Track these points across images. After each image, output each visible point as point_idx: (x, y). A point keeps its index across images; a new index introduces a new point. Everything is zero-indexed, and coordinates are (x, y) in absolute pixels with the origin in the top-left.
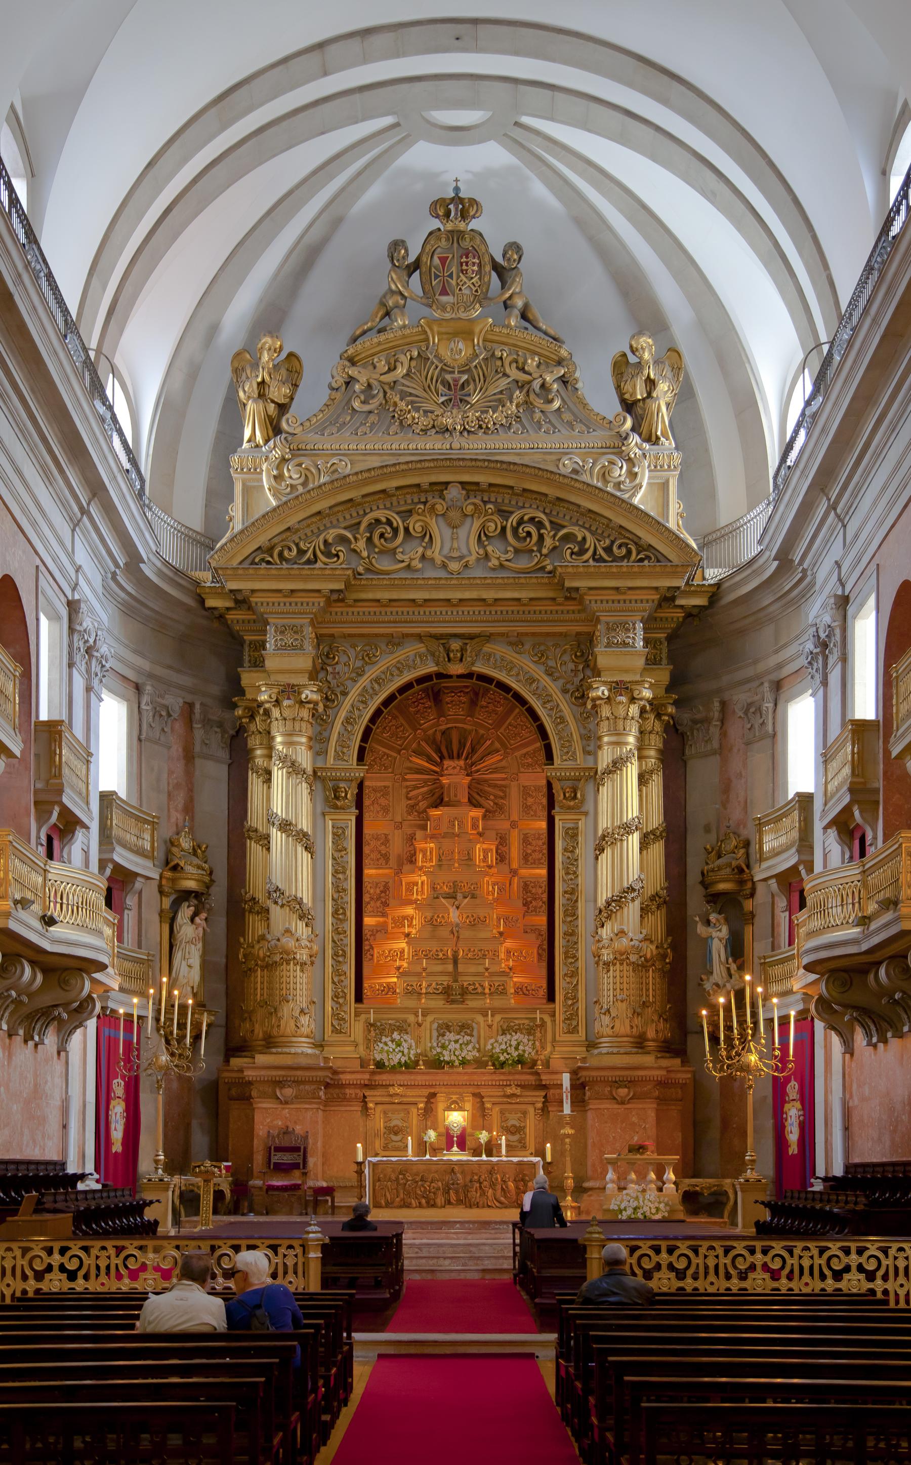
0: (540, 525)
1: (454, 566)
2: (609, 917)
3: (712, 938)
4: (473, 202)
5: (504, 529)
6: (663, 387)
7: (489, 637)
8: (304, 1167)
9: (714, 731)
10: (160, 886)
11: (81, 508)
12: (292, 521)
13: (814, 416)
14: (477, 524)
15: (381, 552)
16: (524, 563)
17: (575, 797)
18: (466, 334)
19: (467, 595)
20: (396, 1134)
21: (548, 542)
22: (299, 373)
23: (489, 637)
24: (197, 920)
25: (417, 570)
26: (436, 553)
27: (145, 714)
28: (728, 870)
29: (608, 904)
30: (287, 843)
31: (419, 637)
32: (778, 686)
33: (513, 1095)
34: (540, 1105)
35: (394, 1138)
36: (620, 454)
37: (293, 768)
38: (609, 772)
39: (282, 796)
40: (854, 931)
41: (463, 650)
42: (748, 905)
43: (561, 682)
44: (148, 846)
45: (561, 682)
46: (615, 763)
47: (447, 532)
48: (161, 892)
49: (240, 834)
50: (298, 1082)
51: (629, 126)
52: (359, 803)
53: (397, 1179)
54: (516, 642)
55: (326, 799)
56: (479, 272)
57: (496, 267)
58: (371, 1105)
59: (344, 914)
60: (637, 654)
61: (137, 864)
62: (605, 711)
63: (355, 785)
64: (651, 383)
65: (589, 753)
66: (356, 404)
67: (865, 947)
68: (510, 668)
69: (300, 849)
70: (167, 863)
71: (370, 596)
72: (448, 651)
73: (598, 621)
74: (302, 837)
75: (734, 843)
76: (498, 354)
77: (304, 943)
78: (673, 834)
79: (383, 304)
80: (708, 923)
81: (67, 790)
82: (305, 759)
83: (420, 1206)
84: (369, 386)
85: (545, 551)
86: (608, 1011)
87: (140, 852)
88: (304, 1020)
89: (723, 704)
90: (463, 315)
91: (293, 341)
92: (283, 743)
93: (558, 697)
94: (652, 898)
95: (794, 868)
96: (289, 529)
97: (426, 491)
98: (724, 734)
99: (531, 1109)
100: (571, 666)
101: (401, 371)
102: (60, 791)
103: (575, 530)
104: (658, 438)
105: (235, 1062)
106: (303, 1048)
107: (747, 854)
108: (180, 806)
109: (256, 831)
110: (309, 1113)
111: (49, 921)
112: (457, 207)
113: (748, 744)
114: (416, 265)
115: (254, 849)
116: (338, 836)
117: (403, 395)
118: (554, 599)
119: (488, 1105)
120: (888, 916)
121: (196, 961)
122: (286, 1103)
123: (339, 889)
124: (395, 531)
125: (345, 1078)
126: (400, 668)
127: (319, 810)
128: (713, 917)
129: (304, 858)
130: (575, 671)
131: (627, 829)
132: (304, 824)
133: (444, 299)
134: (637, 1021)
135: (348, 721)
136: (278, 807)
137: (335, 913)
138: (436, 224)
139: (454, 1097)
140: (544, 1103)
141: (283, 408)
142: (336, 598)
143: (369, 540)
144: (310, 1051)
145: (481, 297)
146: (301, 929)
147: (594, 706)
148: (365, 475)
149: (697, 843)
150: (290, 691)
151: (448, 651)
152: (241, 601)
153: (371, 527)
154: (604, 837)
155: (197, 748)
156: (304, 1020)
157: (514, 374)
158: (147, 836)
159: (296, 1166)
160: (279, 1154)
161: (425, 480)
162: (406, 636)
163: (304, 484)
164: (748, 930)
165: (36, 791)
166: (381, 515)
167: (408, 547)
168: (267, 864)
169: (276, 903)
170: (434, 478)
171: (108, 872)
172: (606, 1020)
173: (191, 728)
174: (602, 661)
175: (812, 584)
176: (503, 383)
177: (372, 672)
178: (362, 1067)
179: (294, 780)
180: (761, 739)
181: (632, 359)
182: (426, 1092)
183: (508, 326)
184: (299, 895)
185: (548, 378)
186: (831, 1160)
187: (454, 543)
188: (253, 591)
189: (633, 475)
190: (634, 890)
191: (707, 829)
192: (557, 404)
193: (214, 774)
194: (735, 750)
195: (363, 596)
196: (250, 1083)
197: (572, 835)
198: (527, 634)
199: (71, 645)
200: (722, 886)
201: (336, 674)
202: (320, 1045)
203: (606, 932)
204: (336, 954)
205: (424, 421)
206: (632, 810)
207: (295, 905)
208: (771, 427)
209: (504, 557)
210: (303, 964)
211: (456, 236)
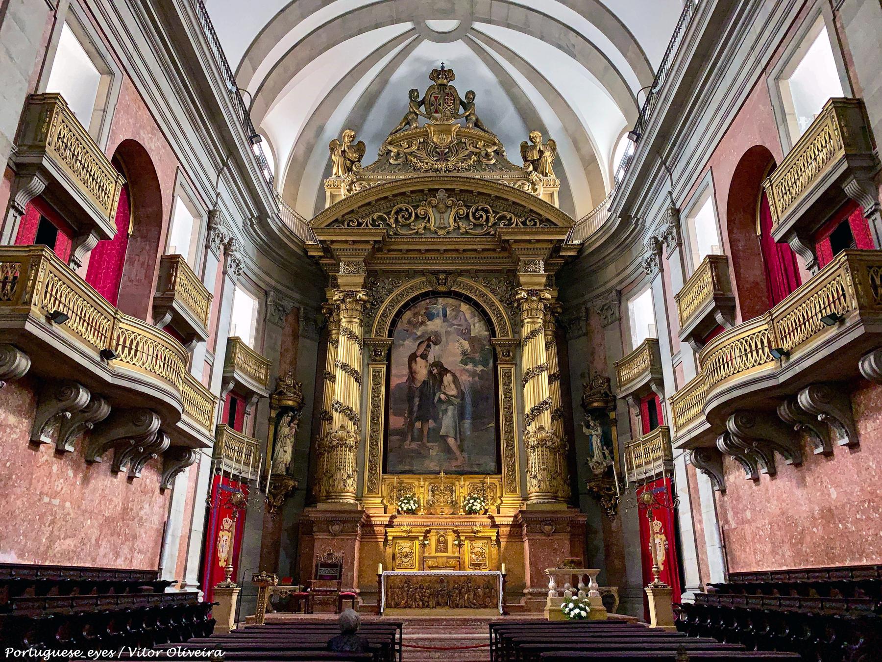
0: (487, 212)
1: (441, 232)
2: (533, 419)
3: (592, 435)
4: (450, 71)
5: (468, 214)
6: (547, 154)
7: (461, 273)
8: (340, 578)
9: (583, 323)
10: (270, 403)
11: (222, 160)
12: (355, 207)
13: (659, 93)
14: (453, 211)
15: (402, 226)
16: (479, 231)
17: (509, 356)
18: (448, 132)
19: (449, 247)
20: (406, 557)
21: (492, 220)
22: (364, 151)
23: (461, 273)
24: (292, 425)
25: (422, 234)
26: (432, 226)
27: (269, 307)
28: (599, 395)
29: (532, 411)
31: (422, 273)
32: (620, 293)
34: (494, 538)
35: (404, 560)
36: (528, 180)
37: (351, 336)
38: (528, 338)
39: (346, 351)
40: (769, 367)
41: (446, 279)
42: (612, 415)
43: (499, 296)
44: (262, 377)
45: (499, 296)
46: (532, 332)
47: (438, 216)
48: (271, 407)
49: (322, 375)
50: (344, 522)
52: (389, 357)
53: (403, 587)
54: (474, 274)
55: (370, 357)
56: (454, 103)
57: (462, 103)
58: (390, 538)
59: (378, 420)
60: (541, 275)
61: (253, 385)
62: (525, 306)
63: (386, 348)
64: (541, 152)
65: (516, 333)
66: (392, 161)
67: (782, 379)
68: (471, 288)
69: (352, 379)
70: (276, 390)
71: (396, 247)
72: (438, 279)
73: (519, 260)
74: (353, 373)
75: (601, 381)
76: (463, 140)
77: (352, 434)
78: (563, 376)
79: (406, 118)
80: (588, 427)
81: (176, 297)
82: (357, 330)
83: (418, 607)
84: (398, 154)
85: (490, 224)
86: (535, 477)
87: (257, 379)
88: (350, 481)
89: (587, 309)
90: (446, 123)
93: (497, 303)
94: (556, 411)
95: (647, 385)
96: (352, 211)
97: (426, 195)
98: (588, 325)
100: (504, 288)
101: (414, 148)
102: (172, 299)
103: (506, 213)
106: (349, 499)
107: (609, 386)
108: (288, 361)
109: (329, 373)
110: (349, 542)
111: (107, 355)
112: (442, 75)
113: (604, 327)
114: (423, 102)
115: (328, 383)
116: (376, 377)
117: (415, 157)
118: (494, 250)
119: (463, 538)
120: (833, 331)
121: (289, 449)
122: (335, 535)
123: (376, 406)
124: (410, 214)
125: (375, 520)
126: (412, 289)
127: (366, 362)
128: (591, 423)
129: (355, 385)
130: (507, 291)
131: (541, 368)
132: (356, 365)
133: (436, 115)
134: (554, 482)
135: (384, 315)
137: (372, 419)
138: (433, 83)
139: (442, 533)
140: (497, 537)
142: (379, 247)
143: (396, 220)
144: (352, 502)
145: (455, 115)
146: (351, 426)
147: (519, 305)
148: (395, 184)
149: (577, 384)
150: (353, 294)
151: (438, 279)
153: (397, 213)
154: (527, 374)
155: (300, 332)
156: (350, 481)
157: (471, 148)
158: (263, 372)
159: (333, 578)
160: (323, 569)
161: (426, 188)
162: (416, 272)
164: (614, 429)
165: (155, 298)
166: (403, 206)
167: (417, 224)
169: (336, 411)
170: (431, 187)
171: (231, 386)
172: (535, 482)
173: (298, 321)
174: (522, 279)
175: (643, 226)
176: (467, 152)
177: (397, 292)
178: (385, 513)
179: (352, 341)
180: (613, 322)
181: (530, 143)
182: (424, 529)
183: (468, 128)
184: (351, 406)
185: (489, 150)
187: (441, 221)
188: (333, 242)
190: (547, 403)
191: (583, 376)
192: (493, 161)
193: (309, 346)
194: (596, 332)
195: (392, 247)
196: (313, 522)
197: (508, 375)
198: (480, 271)
199: (208, 236)
200: (595, 404)
201: (377, 292)
202: (359, 498)
203: (532, 428)
204: (372, 444)
205: (426, 167)
206: (543, 360)
207: (347, 412)
208: (605, 172)
209: (468, 227)
210: (351, 448)
211: (442, 86)
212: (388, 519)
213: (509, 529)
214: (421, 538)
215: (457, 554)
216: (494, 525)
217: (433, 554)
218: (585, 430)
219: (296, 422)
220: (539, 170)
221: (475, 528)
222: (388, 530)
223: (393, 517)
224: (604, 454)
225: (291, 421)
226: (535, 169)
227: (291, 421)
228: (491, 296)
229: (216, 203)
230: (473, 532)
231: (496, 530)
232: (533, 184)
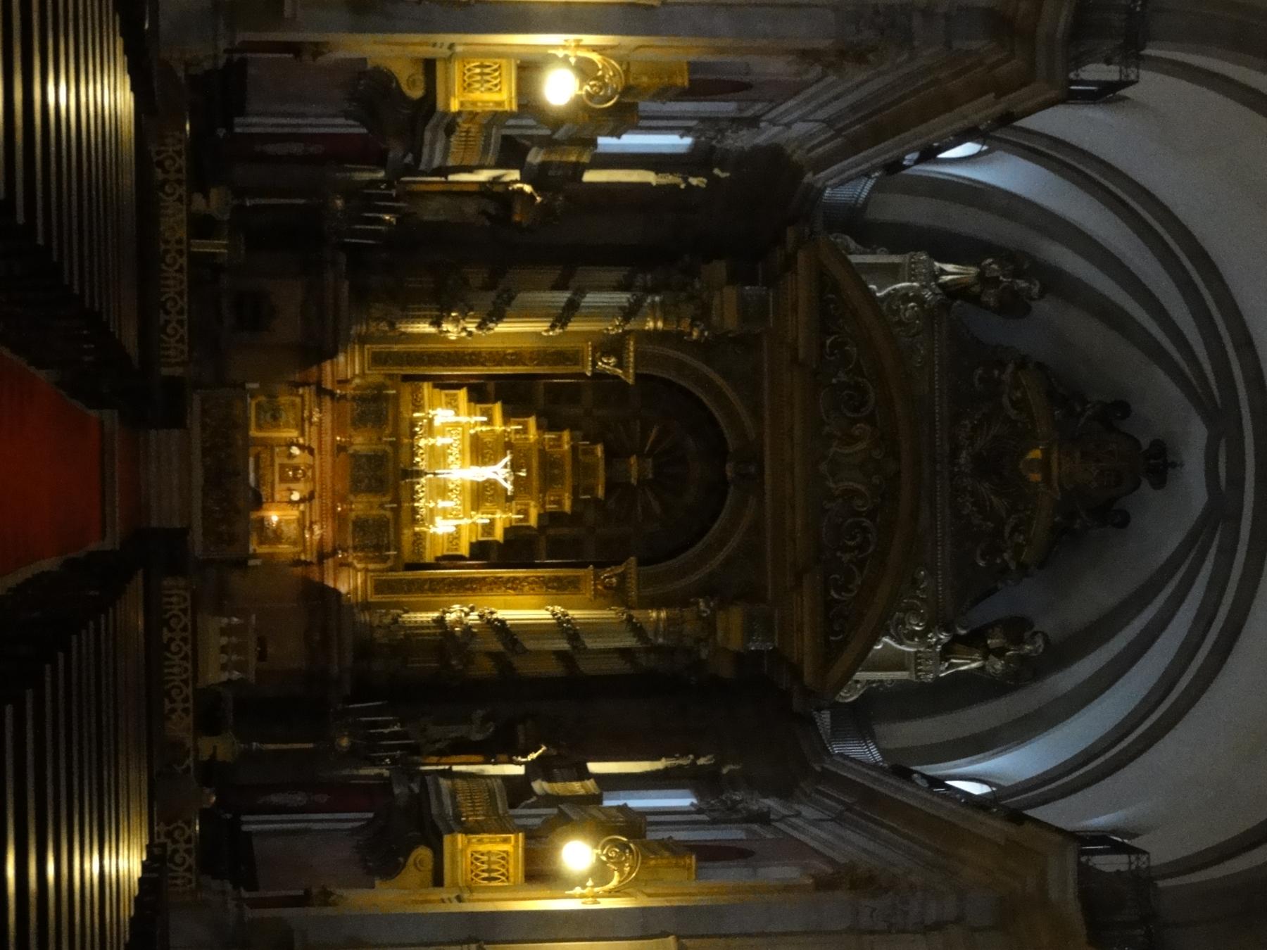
30: (557, 308)
33: (312, 532)
34: (303, 557)
35: (268, 415)
51: (1204, 618)
58: (301, 391)
64: (999, 652)
66: (980, 371)
91: (1045, 308)
92: (653, 301)
99: (299, 549)
104: (947, 660)
105: (342, 258)
119: (302, 507)
125: (327, 366)
133: (1078, 454)
136: (591, 299)
139: (309, 473)
141: (975, 300)
152: (790, 264)
163: (900, 323)
168: (538, 288)
178: (340, 382)
182: (314, 445)
186: (252, 824)
189: (912, 635)
192: (981, 564)
212: (329, 387)
213: (317, 579)
214: (301, 441)
215: (277, 497)
216: (322, 557)
217: (278, 461)
218: (480, 713)
219: (488, 223)
220: (959, 647)
221: (316, 528)
222: (313, 388)
223: (332, 394)
224: (440, 740)
225: (489, 216)
226: (956, 639)
227: (489, 216)
228: (721, 556)
229: (775, 125)
230: (312, 523)
231: (315, 560)
232: (923, 635)
